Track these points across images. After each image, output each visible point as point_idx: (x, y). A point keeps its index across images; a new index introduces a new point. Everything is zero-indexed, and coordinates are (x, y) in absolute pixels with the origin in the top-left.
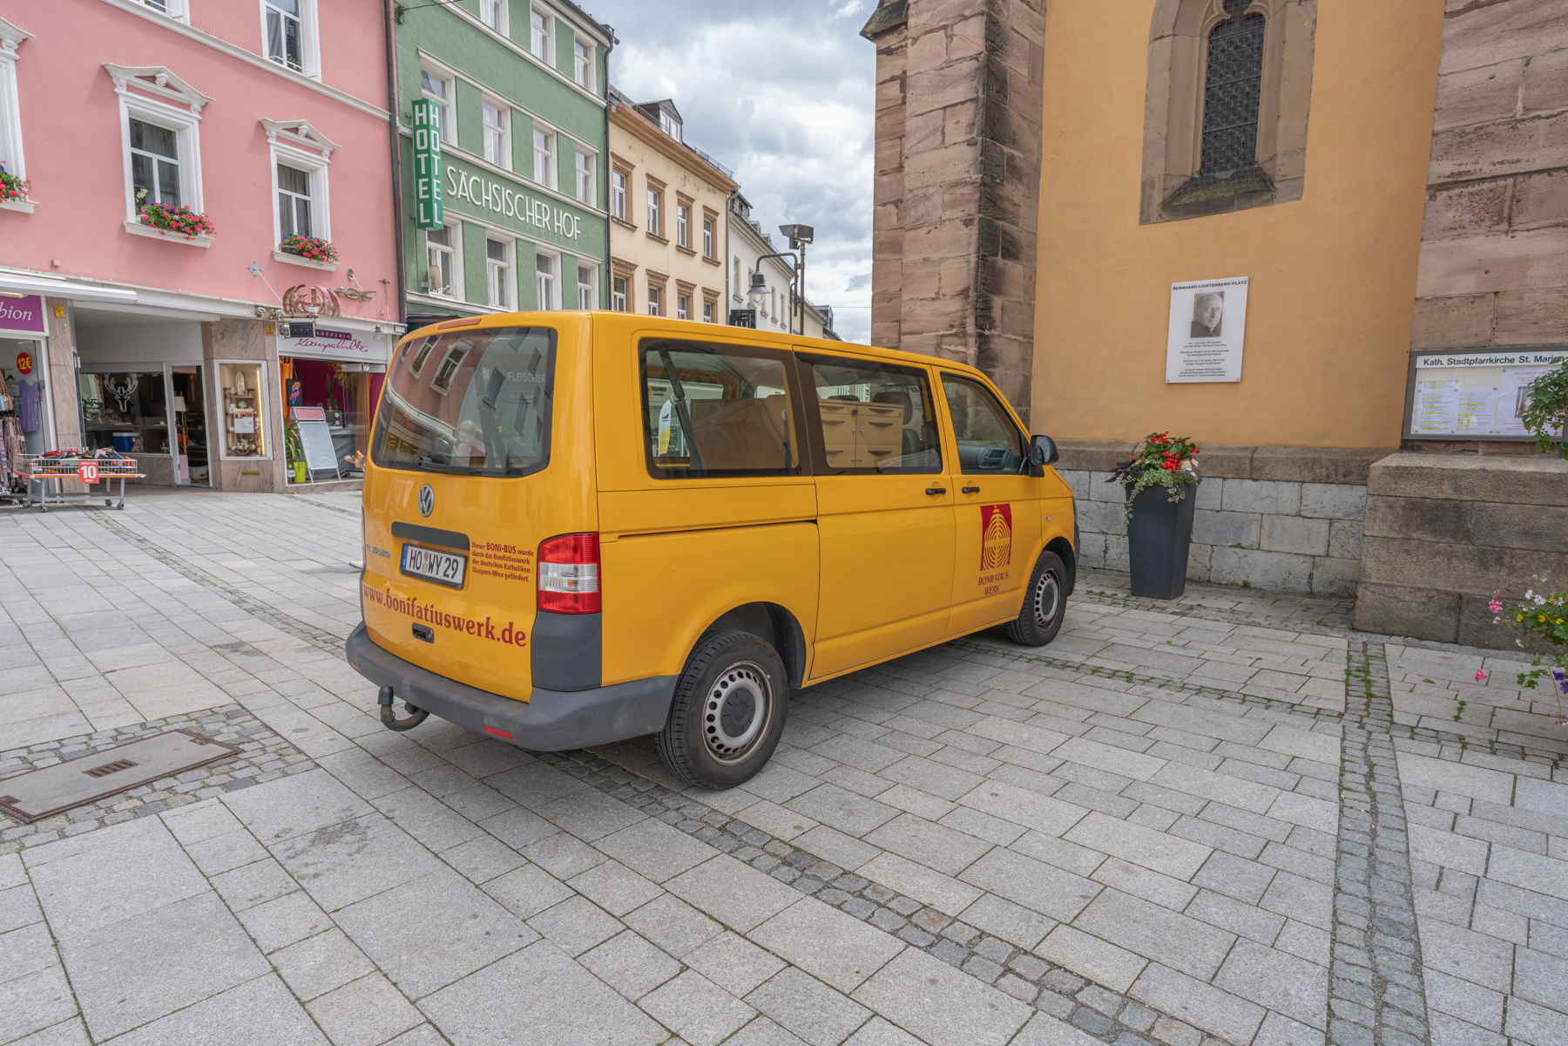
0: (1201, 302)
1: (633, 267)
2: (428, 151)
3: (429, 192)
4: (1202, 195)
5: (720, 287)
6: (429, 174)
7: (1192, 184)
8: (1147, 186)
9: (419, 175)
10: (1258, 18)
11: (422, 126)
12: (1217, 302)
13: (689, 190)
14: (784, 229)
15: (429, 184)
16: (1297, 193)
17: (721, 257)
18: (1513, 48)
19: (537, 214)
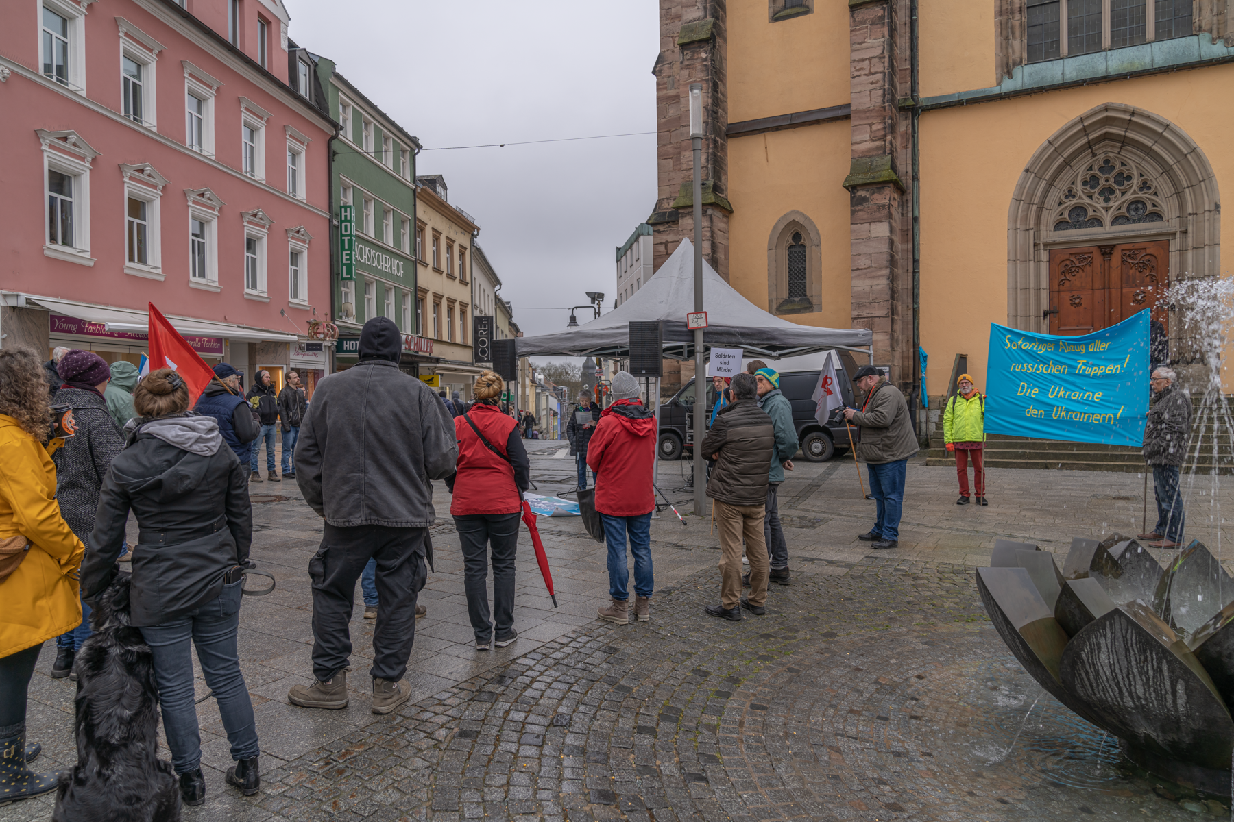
1: (425, 291)
2: (350, 235)
3: (350, 259)
4: (789, 307)
5: (467, 300)
6: (350, 248)
7: (786, 302)
8: (770, 301)
9: (343, 249)
10: (803, 246)
11: (346, 220)
13: (452, 236)
14: (588, 294)
15: (350, 255)
16: (820, 310)
17: (468, 279)
18: (868, 282)
19: (386, 264)
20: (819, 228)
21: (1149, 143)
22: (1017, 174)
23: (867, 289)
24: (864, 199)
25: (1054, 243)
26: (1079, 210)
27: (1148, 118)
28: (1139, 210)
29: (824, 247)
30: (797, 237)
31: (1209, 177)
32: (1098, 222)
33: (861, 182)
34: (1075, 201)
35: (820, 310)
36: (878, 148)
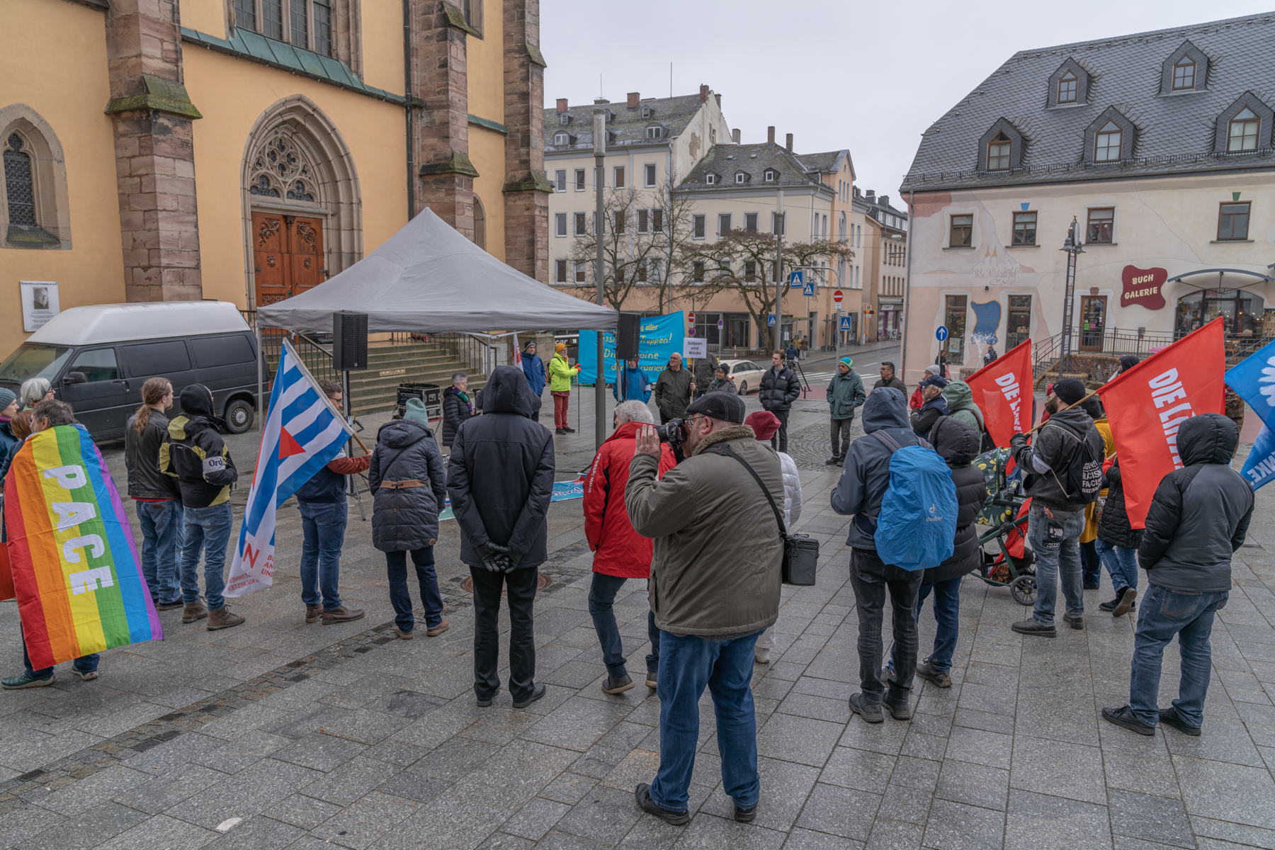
0: (37, 292)
12: (44, 293)
16: (70, 247)
18: (176, 227)
20: (61, 139)
21: (318, 138)
22: (245, 138)
23: (176, 235)
24: (165, 130)
25: (258, 207)
26: (265, 178)
27: (324, 118)
28: (301, 192)
29: (70, 164)
30: (15, 140)
31: (355, 178)
32: (276, 193)
33: (168, 108)
34: (263, 171)
35: (70, 247)
36: (170, 72)
